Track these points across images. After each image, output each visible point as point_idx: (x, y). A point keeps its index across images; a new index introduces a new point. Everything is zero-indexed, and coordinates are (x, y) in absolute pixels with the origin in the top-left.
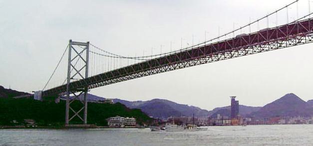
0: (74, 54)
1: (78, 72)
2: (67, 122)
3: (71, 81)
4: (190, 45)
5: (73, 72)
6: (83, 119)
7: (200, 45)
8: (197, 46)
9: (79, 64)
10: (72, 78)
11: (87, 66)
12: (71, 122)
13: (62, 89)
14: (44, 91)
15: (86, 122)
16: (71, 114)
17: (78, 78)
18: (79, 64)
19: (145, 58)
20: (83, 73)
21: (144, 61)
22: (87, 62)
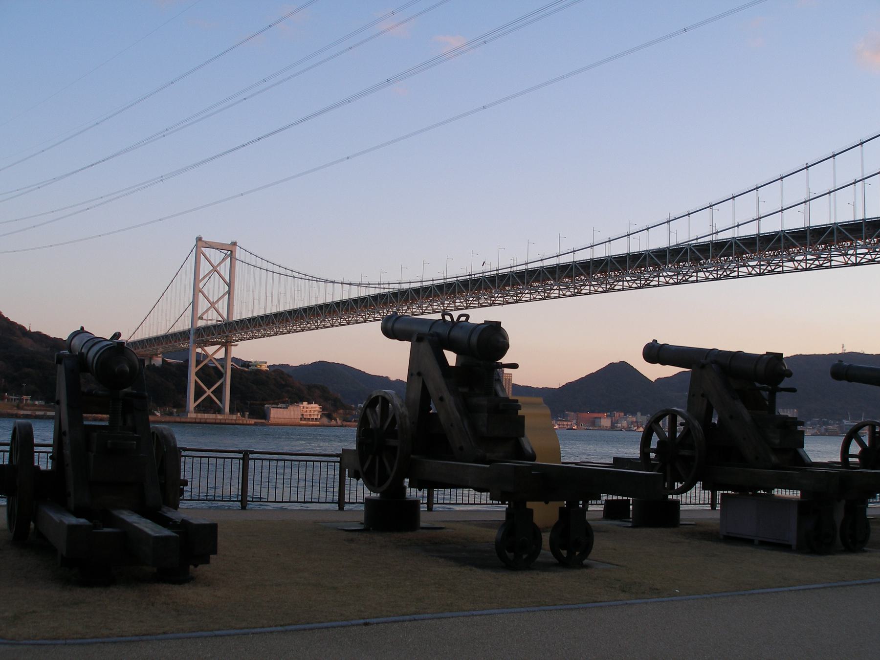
0: (205, 267)
1: (213, 305)
2: (192, 404)
3: (200, 323)
4: (494, 267)
5: (203, 305)
6: (220, 400)
7: (500, 272)
8: (509, 270)
9: (215, 288)
10: (201, 318)
11: (229, 293)
12: (198, 409)
13: (184, 335)
14: (132, 339)
15: (227, 409)
16: (199, 392)
17: (212, 318)
18: (215, 288)
19: (392, 286)
20: (223, 306)
21: (382, 291)
22: (230, 284)
